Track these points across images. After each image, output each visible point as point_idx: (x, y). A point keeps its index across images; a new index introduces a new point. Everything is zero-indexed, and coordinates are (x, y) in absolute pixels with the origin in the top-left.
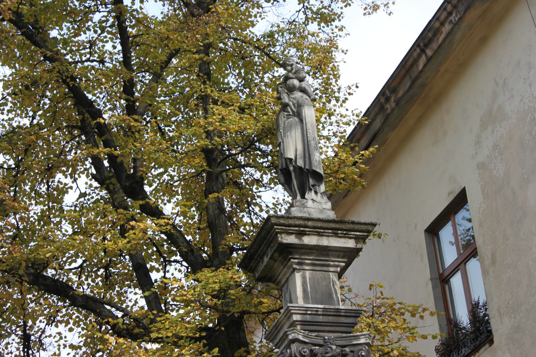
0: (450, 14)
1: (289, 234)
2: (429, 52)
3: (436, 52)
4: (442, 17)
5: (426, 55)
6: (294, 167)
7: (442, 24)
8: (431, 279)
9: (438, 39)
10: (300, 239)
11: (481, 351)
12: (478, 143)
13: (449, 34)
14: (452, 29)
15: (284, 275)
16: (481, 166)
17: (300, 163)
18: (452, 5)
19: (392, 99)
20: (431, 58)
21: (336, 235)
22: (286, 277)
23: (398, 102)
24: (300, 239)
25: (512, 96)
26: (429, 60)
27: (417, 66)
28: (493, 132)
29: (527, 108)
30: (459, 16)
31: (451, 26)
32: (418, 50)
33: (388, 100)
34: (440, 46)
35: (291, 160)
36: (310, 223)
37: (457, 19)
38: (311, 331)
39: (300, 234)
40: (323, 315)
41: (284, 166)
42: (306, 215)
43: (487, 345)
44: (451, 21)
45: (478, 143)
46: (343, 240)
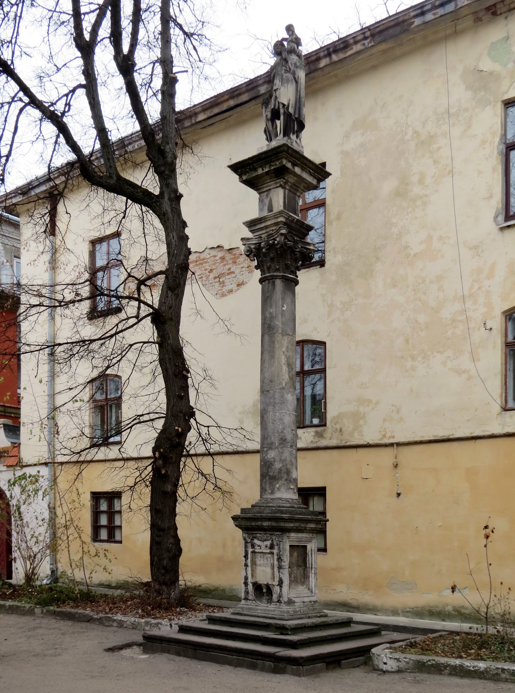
0: (365, 38)
2: (335, 58)
3: (341, 61)
4: (359, 38)
5: (331, 59)
7: (356, 43)
9: (346, 52)
13: (358, 53)
14: (362, 50)
18: (371, 33)
27: (319, 63)
30: (373, 44)
32: (326, 52)
37: (370, 45)
44: (364, 44)
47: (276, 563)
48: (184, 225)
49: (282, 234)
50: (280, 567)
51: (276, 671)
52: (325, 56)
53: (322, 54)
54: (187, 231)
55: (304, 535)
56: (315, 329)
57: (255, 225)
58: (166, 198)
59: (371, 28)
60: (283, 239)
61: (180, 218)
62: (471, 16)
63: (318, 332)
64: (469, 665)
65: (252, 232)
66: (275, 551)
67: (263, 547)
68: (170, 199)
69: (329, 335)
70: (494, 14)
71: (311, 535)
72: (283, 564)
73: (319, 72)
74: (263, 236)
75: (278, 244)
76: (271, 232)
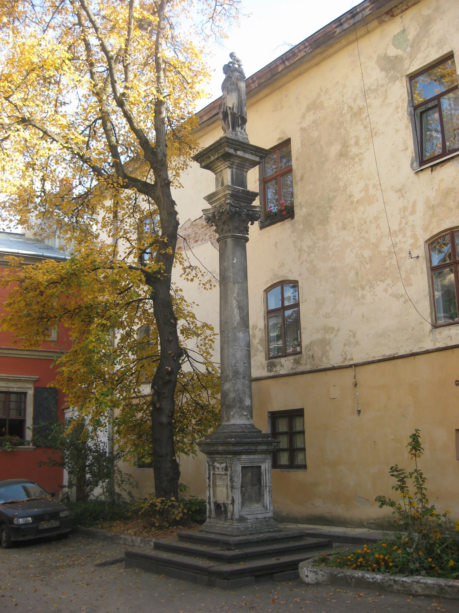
1: (232, 148)
2: (287, 64)
5: (285, 65)
6: (231, 112)
7: (300, 51)
8: (259, 180)
10: (236, 152)
11: (285, 221)
12: (303, 117)
14: (305, 56)
15: (220, 168)
16: (303, 130)
17: (235, 111)
19: (257, 82)
20: (288, 66)
21: (252, 154)
22: (221, 169)
23: (259, 85)
24: (236, 152)
25: (330, 99)
26: (286, 68)
28: (314, 114)
29: (338, 107)
31: (305, 54)
32: (281, 61)
33: (254, 82)
34: (295, 63)
35: (230, 108)
36: (242, 145)
37: (309, 51)
38: (236, 200)
39: (236, 150)
40: (241, 193)
41: (225, 111)
42: (237, 139)
43: (290, 219)
45: (303, 117)
46: (254, 156)
47: (229, 483)
48: (173, 203)
49: (228, 204)
50: (232, 487)
51: (210, 585)
52: (281, 64)
53: (278, 63)
54: (177, 208)
55: (256, 456)
56: (290, 271)
57: (211, 199)
58: (159, 186)
59: (308, 40)
60: (228, 208)
61: (169, 199)
62: (376, 20)
63: (292, 273)
64: (369, 576)
65: (211, 203)
66: (228, 473)
67: (220, 469)
68: (162, 186)
69: (300, 275)
70: (393, 16)
71: (264, 456)
72: (235, 484)
73: (279, 75)
74: (217, 206)
75: (225, 211)
76: (223, 202)
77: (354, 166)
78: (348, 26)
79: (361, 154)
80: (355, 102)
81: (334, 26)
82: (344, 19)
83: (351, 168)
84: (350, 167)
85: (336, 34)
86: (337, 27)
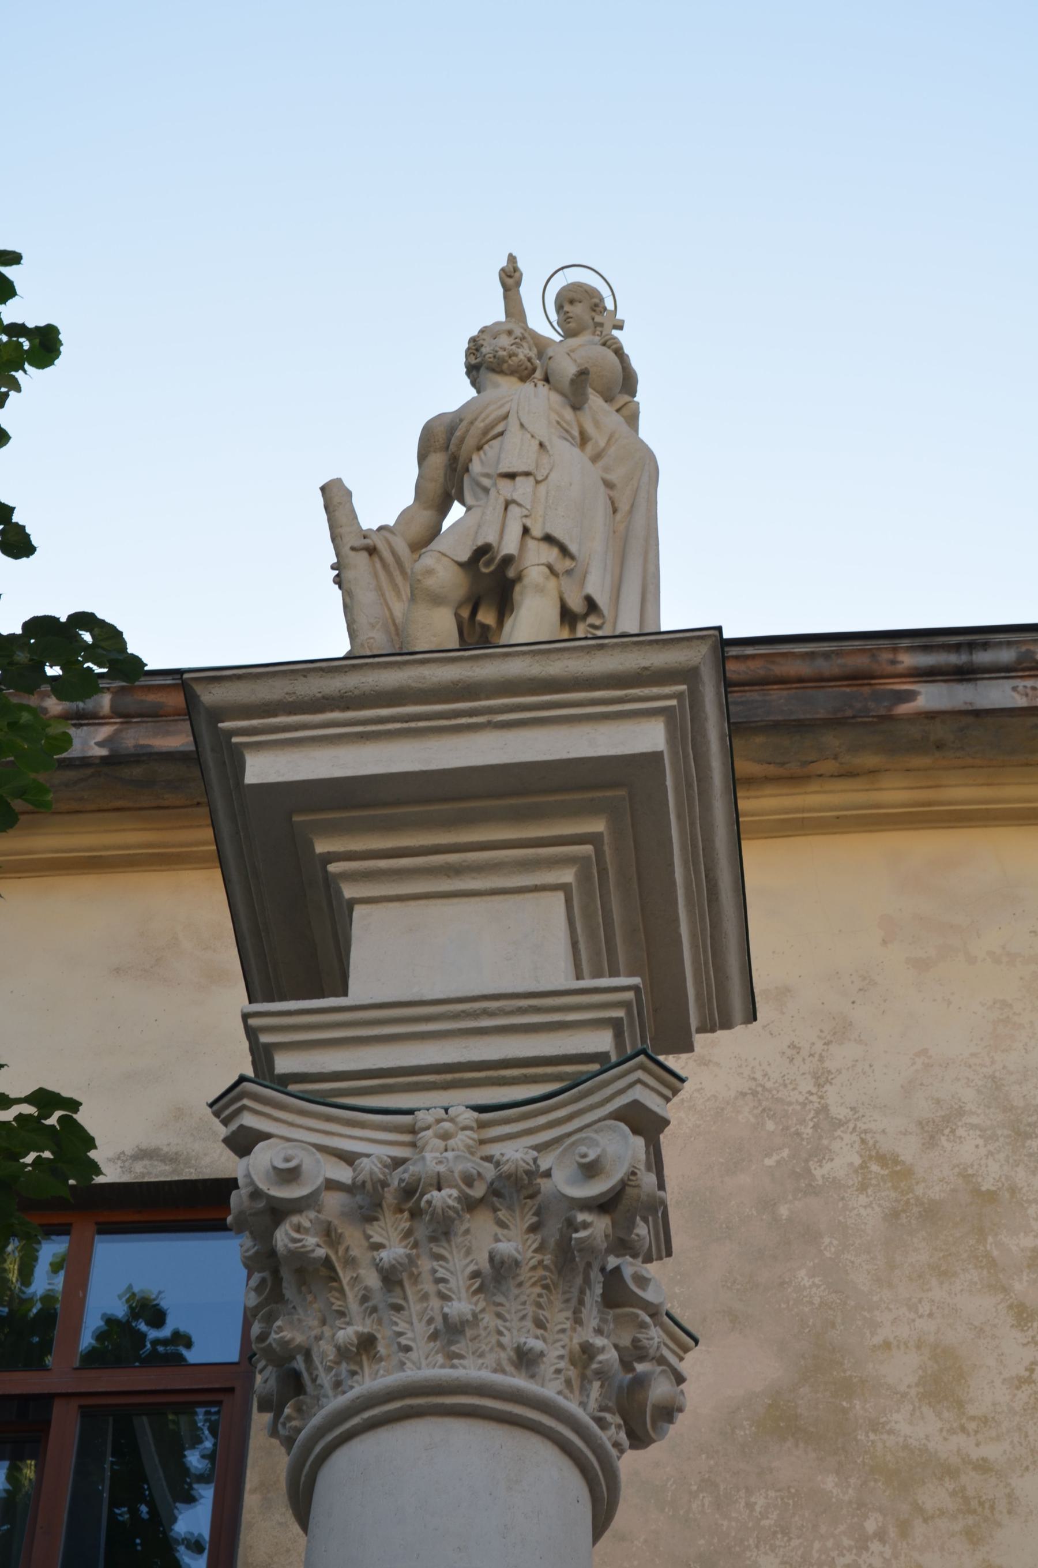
23: (116, 761)
77: (904, 1529)
78: (1021, 702)
79: (983, 1467)
80: (931, 1142)
81: (908, 660)
82: (1006, 656)
83: (881, 1536)
84: (871, 1526)
85: (904, 708)
86: (929, 675)
